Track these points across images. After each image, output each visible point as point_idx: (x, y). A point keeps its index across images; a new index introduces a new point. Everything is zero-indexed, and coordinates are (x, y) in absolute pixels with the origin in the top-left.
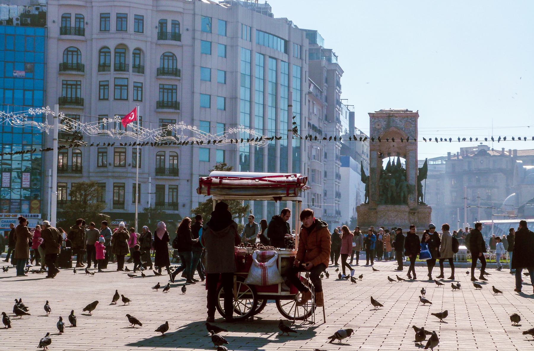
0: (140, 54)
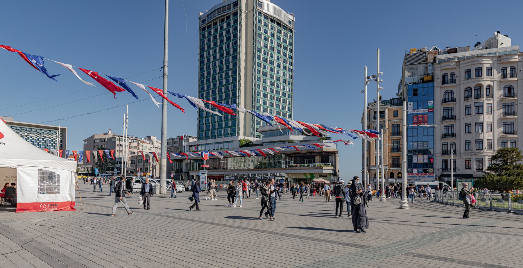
0: (489, 88)
